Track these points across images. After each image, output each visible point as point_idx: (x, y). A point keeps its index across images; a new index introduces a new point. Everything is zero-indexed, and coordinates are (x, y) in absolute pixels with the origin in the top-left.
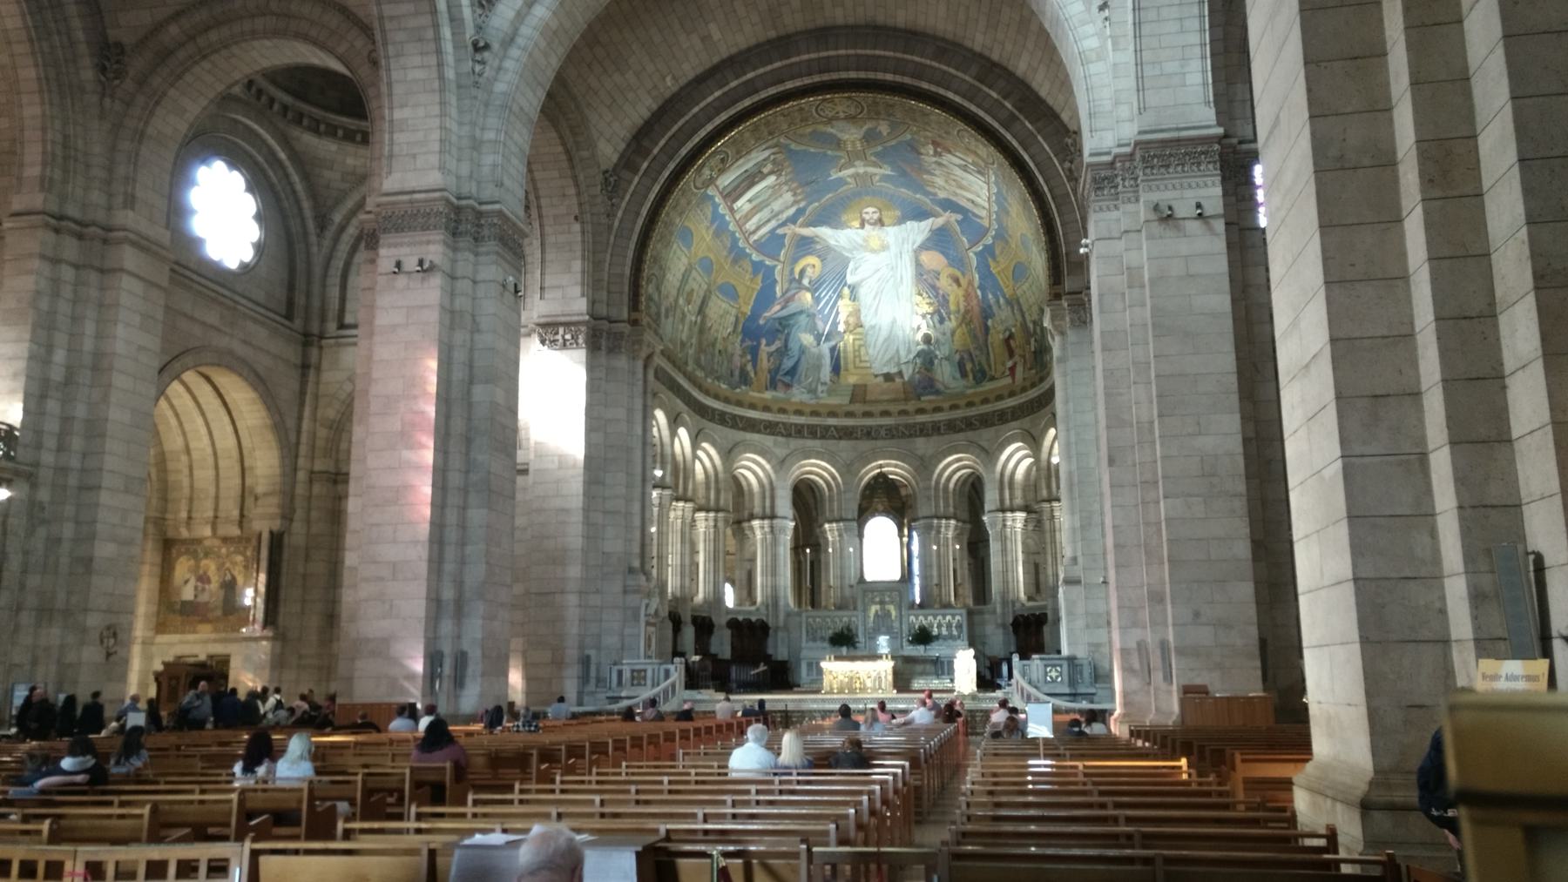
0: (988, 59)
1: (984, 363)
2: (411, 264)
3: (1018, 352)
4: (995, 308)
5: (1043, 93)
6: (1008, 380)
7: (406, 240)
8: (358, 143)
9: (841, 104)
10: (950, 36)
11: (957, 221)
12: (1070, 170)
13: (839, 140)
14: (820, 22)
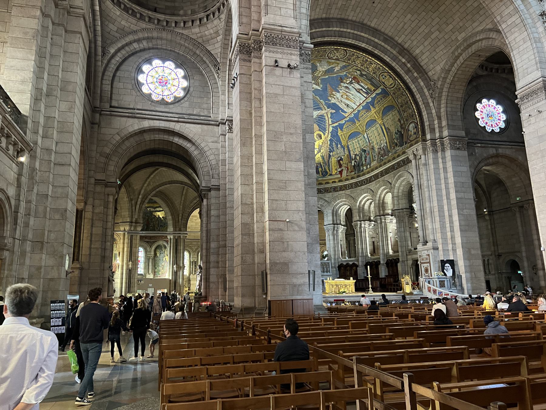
0: (402, 47)
1: (327, 168)
2: (284, 63)
3: (344, 165)
4: (335, 149)
5: (422, 64)
6: (339, 176)
7: (279, 50)
8: (129, 14)
9: (340, 52)
10: (390, 34)
11: (331, 113)
12: (432, 94)
13: (317, 70)
14: (343, 17)
